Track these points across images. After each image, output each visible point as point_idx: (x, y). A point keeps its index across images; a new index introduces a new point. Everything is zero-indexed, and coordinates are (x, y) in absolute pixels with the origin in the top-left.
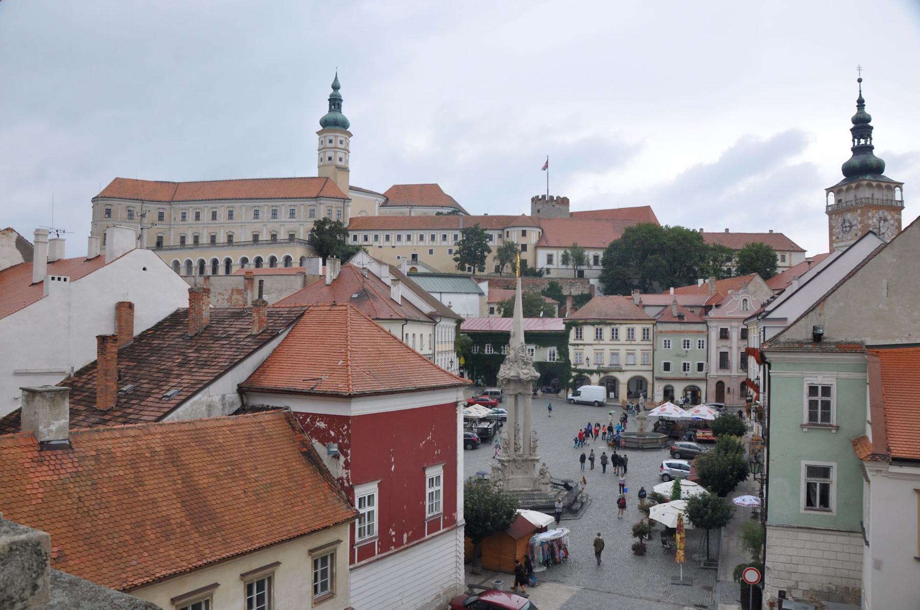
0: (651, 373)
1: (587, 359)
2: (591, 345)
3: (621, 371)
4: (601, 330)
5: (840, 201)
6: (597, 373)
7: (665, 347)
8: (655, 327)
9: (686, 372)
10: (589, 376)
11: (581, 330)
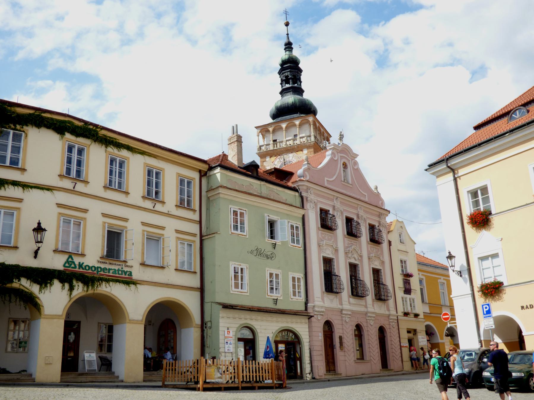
0: (198, 294)
1: (39, 229)
2: (49, 189)
3: (129, 282)
4: (80, 152)
5: (275, 141)
6: (62, 281)
7: (236, 228)
8: (204, 180)
9: (275, 295)
10: (35, 289)
11: (17, 138)
